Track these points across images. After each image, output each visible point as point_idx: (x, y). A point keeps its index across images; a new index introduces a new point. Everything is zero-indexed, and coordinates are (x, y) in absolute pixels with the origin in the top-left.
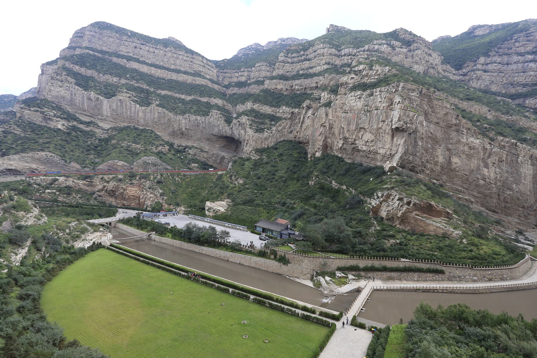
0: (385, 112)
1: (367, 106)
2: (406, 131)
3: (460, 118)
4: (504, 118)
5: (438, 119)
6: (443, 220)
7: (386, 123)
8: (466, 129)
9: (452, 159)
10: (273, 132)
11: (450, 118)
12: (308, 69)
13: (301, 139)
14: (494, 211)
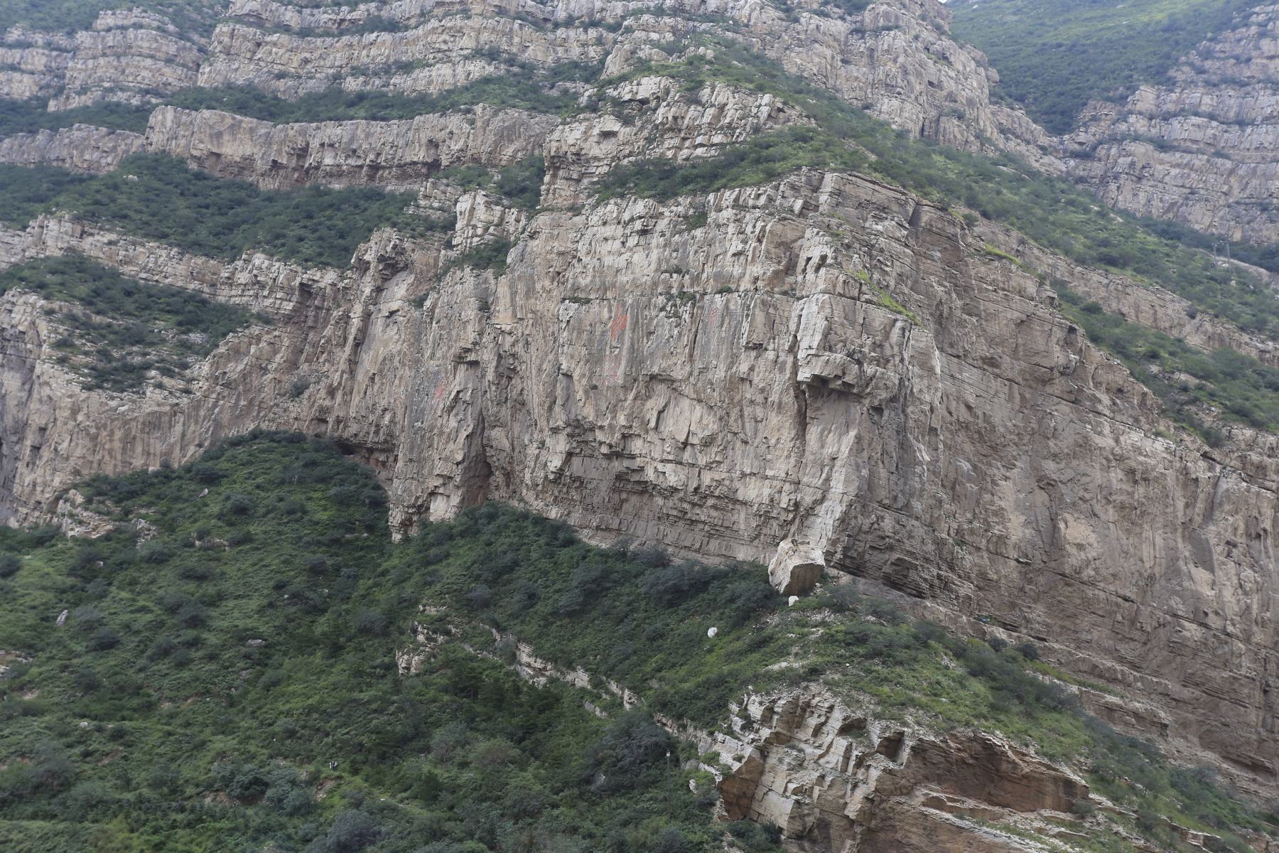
0: (764, 303)
1: (678, 271)
2: (859, 397)
3: (1082, 341)
5: (991, 342)
6: (1048, 820)
7: (770, 355)
8: (1108, 390)
9: (1062, 525)
10: (195, 386)
11: (1040, 344)
12: (387, 70)
13: (353, 428)
14: (1255, 767)
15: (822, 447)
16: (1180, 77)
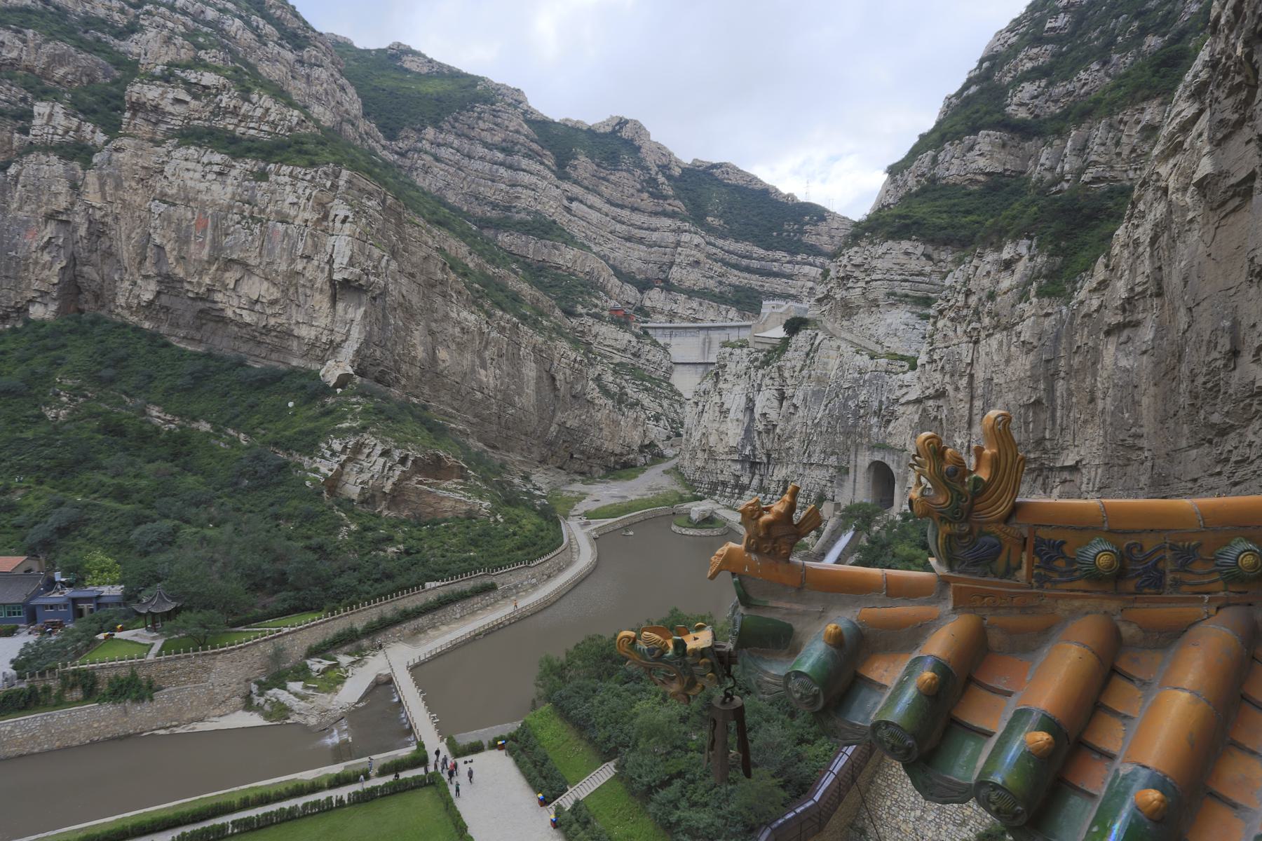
0: (312, 234)
1: (249, 203)
2: (366, 292)
3: (448, 269)
4: (491, 270)
5: (413, 265)
6: (456, 483)
7: (315, 263)
11: (432, 269)
16: (445, 127)
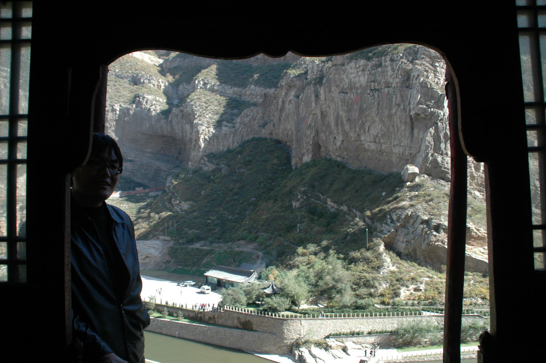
1: (373, 82)
13: (281, 136)
15: (419, 135)
